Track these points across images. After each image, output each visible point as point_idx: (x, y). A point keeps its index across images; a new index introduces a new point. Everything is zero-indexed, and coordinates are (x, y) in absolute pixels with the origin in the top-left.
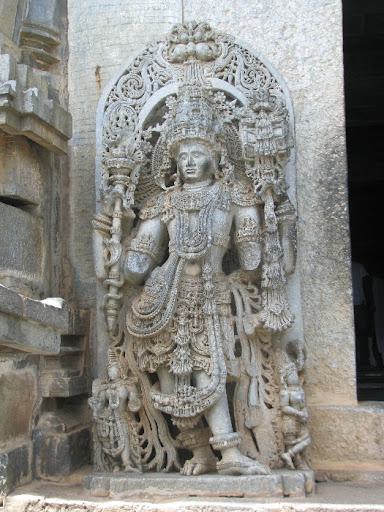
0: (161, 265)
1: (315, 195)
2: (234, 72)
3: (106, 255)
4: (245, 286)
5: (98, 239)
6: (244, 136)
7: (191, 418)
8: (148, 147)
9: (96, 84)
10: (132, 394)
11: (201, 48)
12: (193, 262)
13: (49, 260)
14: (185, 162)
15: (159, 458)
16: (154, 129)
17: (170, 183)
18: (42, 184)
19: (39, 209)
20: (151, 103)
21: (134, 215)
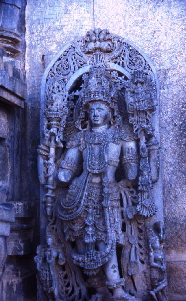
0: (78, 176)
1: (172, 133)
3: (45, 171)
5: (41, 160)
6: (130, 99)
7: (95, 270)
8: (72, 104)
9: (42, 66)
10: (60, 255)
11: (105, 45)
12: (96, 175)
13: (12, 173)
15: (77, 293)
18: (9, 127)
19: (6, 142)
20: (73, 78)
21: (63, 146)
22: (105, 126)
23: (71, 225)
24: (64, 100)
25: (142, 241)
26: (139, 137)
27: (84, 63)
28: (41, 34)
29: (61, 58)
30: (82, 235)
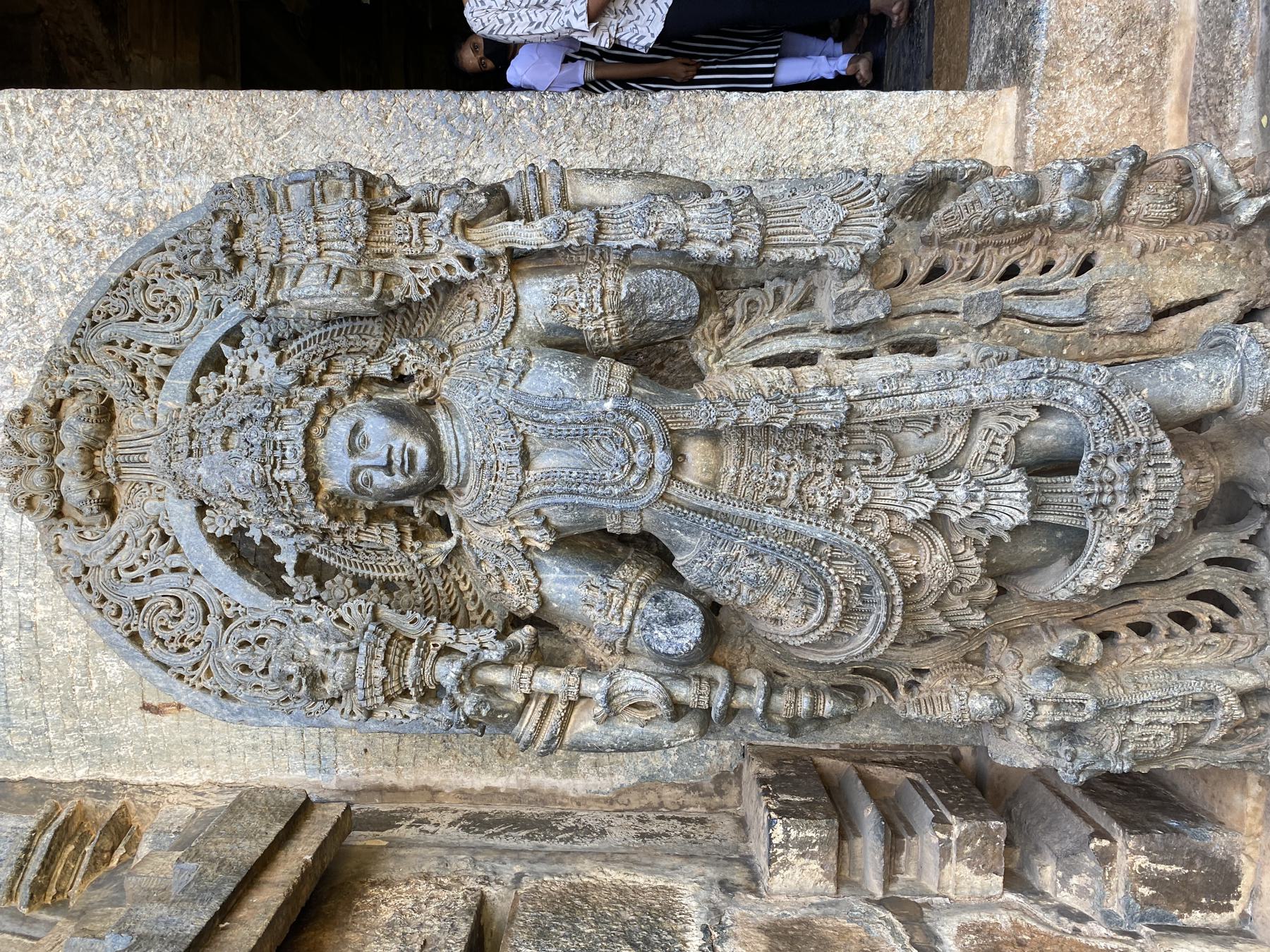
3: (643, 716)
8: (338, 586)
12: (678, 459)
14: (381, 479)
16: (290, 568)
17: (443, 525)
19: (492, 891)
21: (528, 629)
22: (441, 426)
23: (924, 590)
24: (305, 620)
25: (986, 263)
26: (497, 249)
27: (158, 526)
28: (54, 716)
29: (128, 628)
30: (976, 543)
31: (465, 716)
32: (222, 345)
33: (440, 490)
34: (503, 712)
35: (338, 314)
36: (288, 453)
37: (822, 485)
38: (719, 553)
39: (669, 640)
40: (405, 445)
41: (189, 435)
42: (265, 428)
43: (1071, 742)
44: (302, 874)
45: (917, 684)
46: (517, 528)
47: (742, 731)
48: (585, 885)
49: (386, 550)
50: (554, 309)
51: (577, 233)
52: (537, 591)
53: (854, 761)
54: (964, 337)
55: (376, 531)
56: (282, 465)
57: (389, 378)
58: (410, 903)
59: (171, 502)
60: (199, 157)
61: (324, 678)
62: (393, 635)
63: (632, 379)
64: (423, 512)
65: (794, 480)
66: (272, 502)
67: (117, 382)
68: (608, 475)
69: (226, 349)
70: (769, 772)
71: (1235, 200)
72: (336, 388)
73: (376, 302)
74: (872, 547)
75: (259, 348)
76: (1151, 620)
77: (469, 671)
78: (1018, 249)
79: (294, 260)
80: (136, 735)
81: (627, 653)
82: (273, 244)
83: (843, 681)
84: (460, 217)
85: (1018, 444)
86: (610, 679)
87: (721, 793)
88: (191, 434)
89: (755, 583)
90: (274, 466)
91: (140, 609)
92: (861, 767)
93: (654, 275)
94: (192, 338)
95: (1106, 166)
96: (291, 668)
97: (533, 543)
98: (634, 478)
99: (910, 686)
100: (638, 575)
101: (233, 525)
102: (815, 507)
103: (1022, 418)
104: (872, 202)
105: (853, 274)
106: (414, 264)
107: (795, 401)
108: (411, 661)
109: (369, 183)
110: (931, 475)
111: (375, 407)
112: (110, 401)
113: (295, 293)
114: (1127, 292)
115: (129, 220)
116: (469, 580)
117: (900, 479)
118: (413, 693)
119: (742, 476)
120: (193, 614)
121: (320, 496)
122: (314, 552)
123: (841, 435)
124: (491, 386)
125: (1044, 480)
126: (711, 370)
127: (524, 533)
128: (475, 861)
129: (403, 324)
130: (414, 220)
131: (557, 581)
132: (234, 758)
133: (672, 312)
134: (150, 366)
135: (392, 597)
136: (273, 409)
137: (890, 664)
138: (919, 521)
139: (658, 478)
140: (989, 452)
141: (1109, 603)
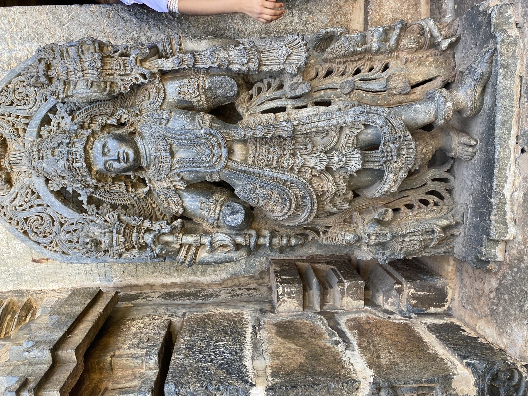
2: (18, 117)
3: (225, 250)
4: (254, 98)
8: (104, 208)
12: (231, 151)
14: (116, 165)
16: (85, 202)
17: (143, 181)
19: (174, 319)
21: (179, 220)
22: (138, 142)
23: (325, 196)
24: (92, 221)
25: (348, 68)
27: (30, 188)
29: (22, 229)
31: (156, 254)
32: (49, 114)
33: (141, 168)
34: (172, 252)
35: (94, 100)
36: (78, 156)
37: (286, 159)
38: (249, 187)
39: (232, 221)
40: (124, 151)
41: (38, 151)
42: (68, 147)
43: (383, 249)
44: (99, 317)
45: (327, 232)
46: (171, 181)
47: (265, 253)
48: (210, 314)
49: (122, 193)
50: (179, 93)
51: (186, 63)
52: (182, 205)
53: (311, 263)
54: (341, 98)
55: (116, 185)
56: (76, 161)
57: (116, 124)
58: (143, 325)
59: (35, 179)
60: (32, 35)
61: (101, 243)
62: (127, 225)
63: (212, 121)
64: (135, 177)
65: (275, 158)
66: (74, 176)
67: (7, 131)
68: (204, 159)
69: (51, 116)
70: (278, 269)
71: (440, 40)
72: (95, 129)
73: (108, 94)
74: (304, 181)
75: (64, 115)
76: (412, 203)
77: (157, 237)
78: (360, 62)
79: (73, 79)
80: (31, 271)
81: (219, 227)
82: (64, 72)
83: (300, 232)
84: (139, 58)
85: (358, 139)
86: (211, 237)
87: (262, 278)
88: (39, 151)
89: (264, 197)
90: (73, 162)
91: (26, 221)
92: (313, 265)
93: (219, 78)
94: (36, 111)
95: (392, 28)
96: (88, 240)
97: (178, 187)
98: (214, 160)
99: (325, 232)
100: (221, 197)
101: (61, 186)
102: (284, 167)
103: (358, 129)
104: (301, 46)
105: (296, 75)
106: (122, 78)
107: (273, 127)
108: (134, 235)
109: (101, 46)
110: (326, 153)
111: (112, 136)
112: (5, 139)
113: (75, 92)
114: (401, 78)
115: (5, 63)
116: (156, 203)
117: (314, 155)
118: (136, 247)
119: (256, 157)
120: (48, 222)
121: (93, 173)
122: (94, 195)
123: (293, 139)
124: (156, 126)
125: (368, 152)
126: (245, 116)
127: (174, 183)
128: (167, 309)
129: (121, 102)
130: (120, 60)
131: (189, 201)
132: (71, 278)
133: (227, 93)
134: (20, 124)
135: (127, 211)
136: (70, 139)
137: (317, 225)
138: (322, 170)
139: (223, 159)
140: (347, 143)
141: (397, 197)
